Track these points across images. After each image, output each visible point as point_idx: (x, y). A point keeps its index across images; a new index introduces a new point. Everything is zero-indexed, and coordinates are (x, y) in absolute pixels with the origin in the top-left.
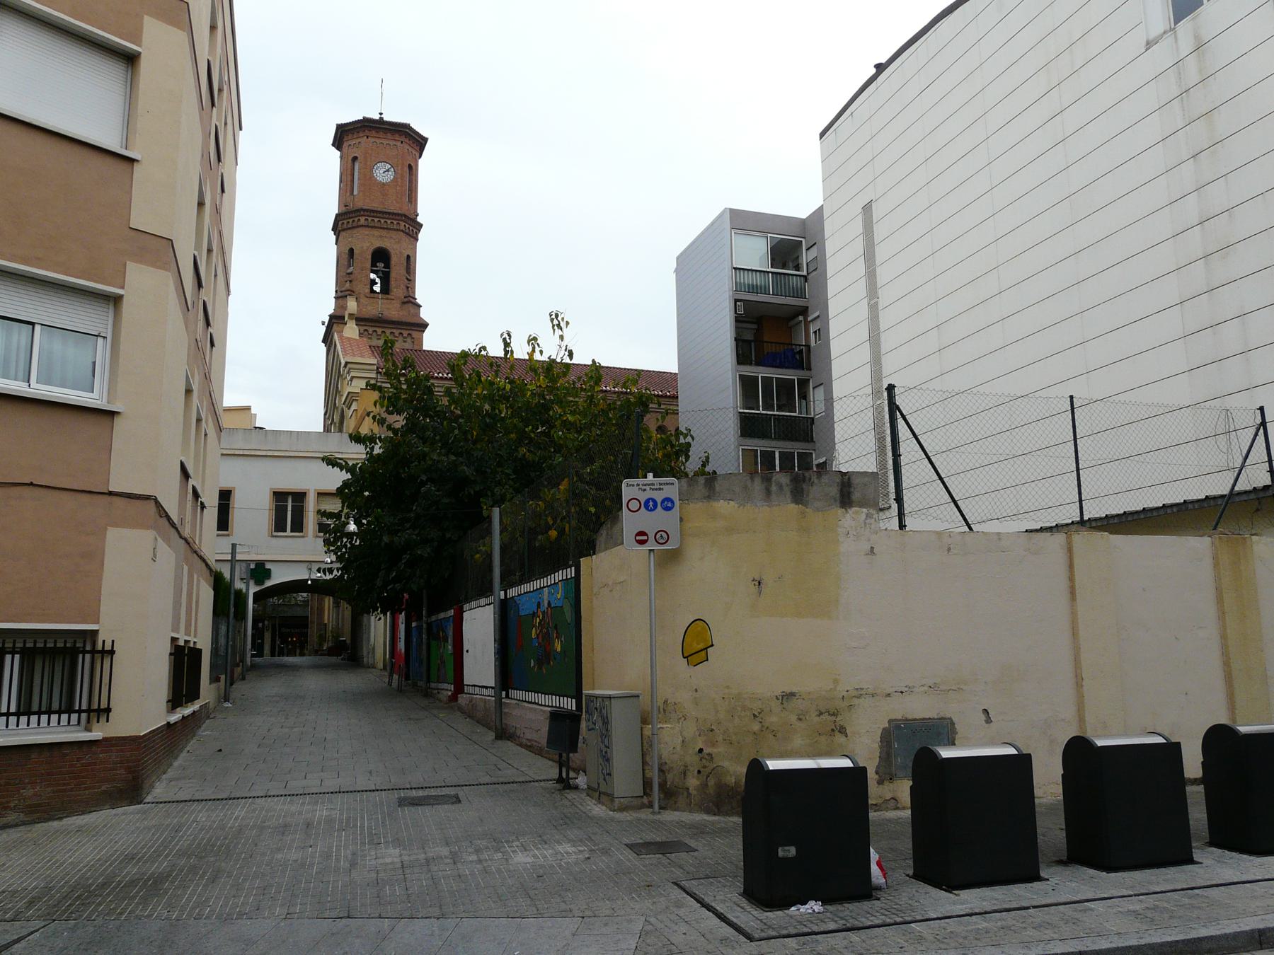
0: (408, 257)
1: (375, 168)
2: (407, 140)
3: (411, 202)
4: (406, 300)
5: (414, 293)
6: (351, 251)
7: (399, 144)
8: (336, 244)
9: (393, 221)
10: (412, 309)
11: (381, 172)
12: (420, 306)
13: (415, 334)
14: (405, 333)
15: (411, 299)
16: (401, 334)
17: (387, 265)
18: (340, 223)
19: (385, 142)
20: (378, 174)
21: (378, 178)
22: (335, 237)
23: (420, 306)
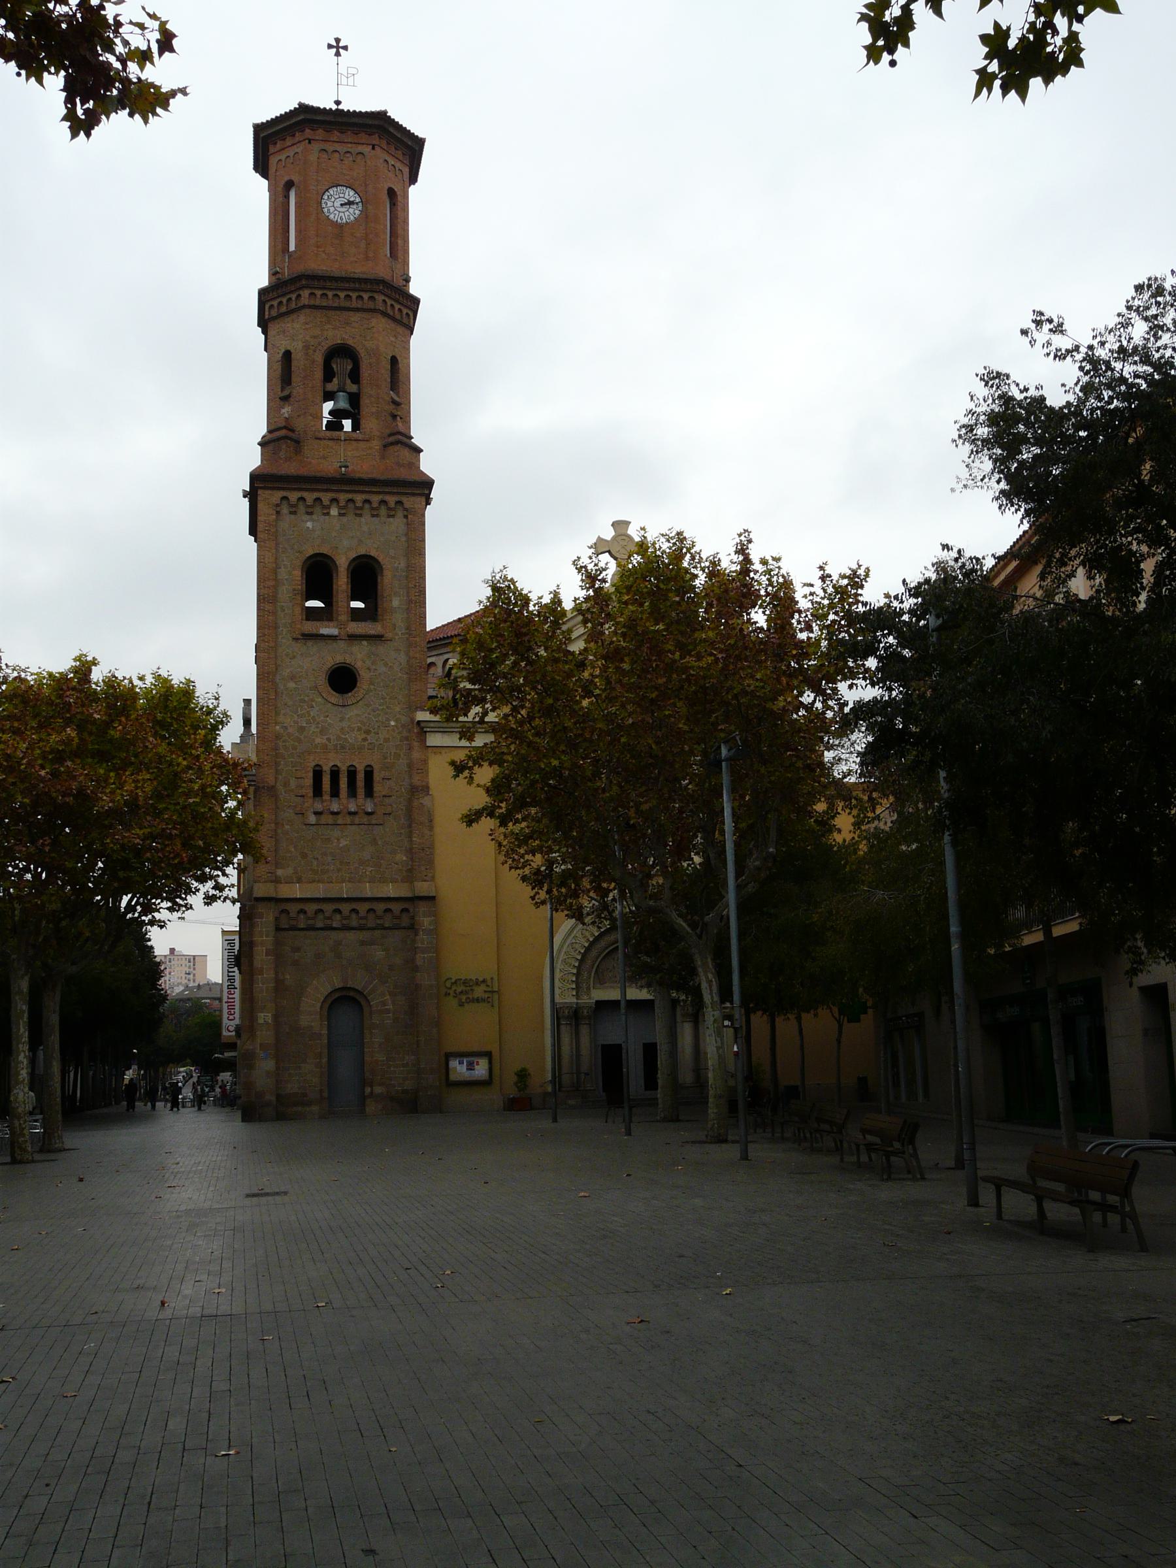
0: (394, 361)
1: (325, 197)
4: (392, 439)
6: (287, 355)
7: (366, 149)
8: (266, 350)
9: (362, 294)
10: (406, 453)
11: (337, 204)
12: (418, 451)
13: (408, 502)
14: (392, 500)
15: (400, 437)
16: (383, 502)
17: (355, 376)
19: (341, 148)
20: (332, 209)
21: (332, 217)
22: (263, 336)
23: (418, 451)
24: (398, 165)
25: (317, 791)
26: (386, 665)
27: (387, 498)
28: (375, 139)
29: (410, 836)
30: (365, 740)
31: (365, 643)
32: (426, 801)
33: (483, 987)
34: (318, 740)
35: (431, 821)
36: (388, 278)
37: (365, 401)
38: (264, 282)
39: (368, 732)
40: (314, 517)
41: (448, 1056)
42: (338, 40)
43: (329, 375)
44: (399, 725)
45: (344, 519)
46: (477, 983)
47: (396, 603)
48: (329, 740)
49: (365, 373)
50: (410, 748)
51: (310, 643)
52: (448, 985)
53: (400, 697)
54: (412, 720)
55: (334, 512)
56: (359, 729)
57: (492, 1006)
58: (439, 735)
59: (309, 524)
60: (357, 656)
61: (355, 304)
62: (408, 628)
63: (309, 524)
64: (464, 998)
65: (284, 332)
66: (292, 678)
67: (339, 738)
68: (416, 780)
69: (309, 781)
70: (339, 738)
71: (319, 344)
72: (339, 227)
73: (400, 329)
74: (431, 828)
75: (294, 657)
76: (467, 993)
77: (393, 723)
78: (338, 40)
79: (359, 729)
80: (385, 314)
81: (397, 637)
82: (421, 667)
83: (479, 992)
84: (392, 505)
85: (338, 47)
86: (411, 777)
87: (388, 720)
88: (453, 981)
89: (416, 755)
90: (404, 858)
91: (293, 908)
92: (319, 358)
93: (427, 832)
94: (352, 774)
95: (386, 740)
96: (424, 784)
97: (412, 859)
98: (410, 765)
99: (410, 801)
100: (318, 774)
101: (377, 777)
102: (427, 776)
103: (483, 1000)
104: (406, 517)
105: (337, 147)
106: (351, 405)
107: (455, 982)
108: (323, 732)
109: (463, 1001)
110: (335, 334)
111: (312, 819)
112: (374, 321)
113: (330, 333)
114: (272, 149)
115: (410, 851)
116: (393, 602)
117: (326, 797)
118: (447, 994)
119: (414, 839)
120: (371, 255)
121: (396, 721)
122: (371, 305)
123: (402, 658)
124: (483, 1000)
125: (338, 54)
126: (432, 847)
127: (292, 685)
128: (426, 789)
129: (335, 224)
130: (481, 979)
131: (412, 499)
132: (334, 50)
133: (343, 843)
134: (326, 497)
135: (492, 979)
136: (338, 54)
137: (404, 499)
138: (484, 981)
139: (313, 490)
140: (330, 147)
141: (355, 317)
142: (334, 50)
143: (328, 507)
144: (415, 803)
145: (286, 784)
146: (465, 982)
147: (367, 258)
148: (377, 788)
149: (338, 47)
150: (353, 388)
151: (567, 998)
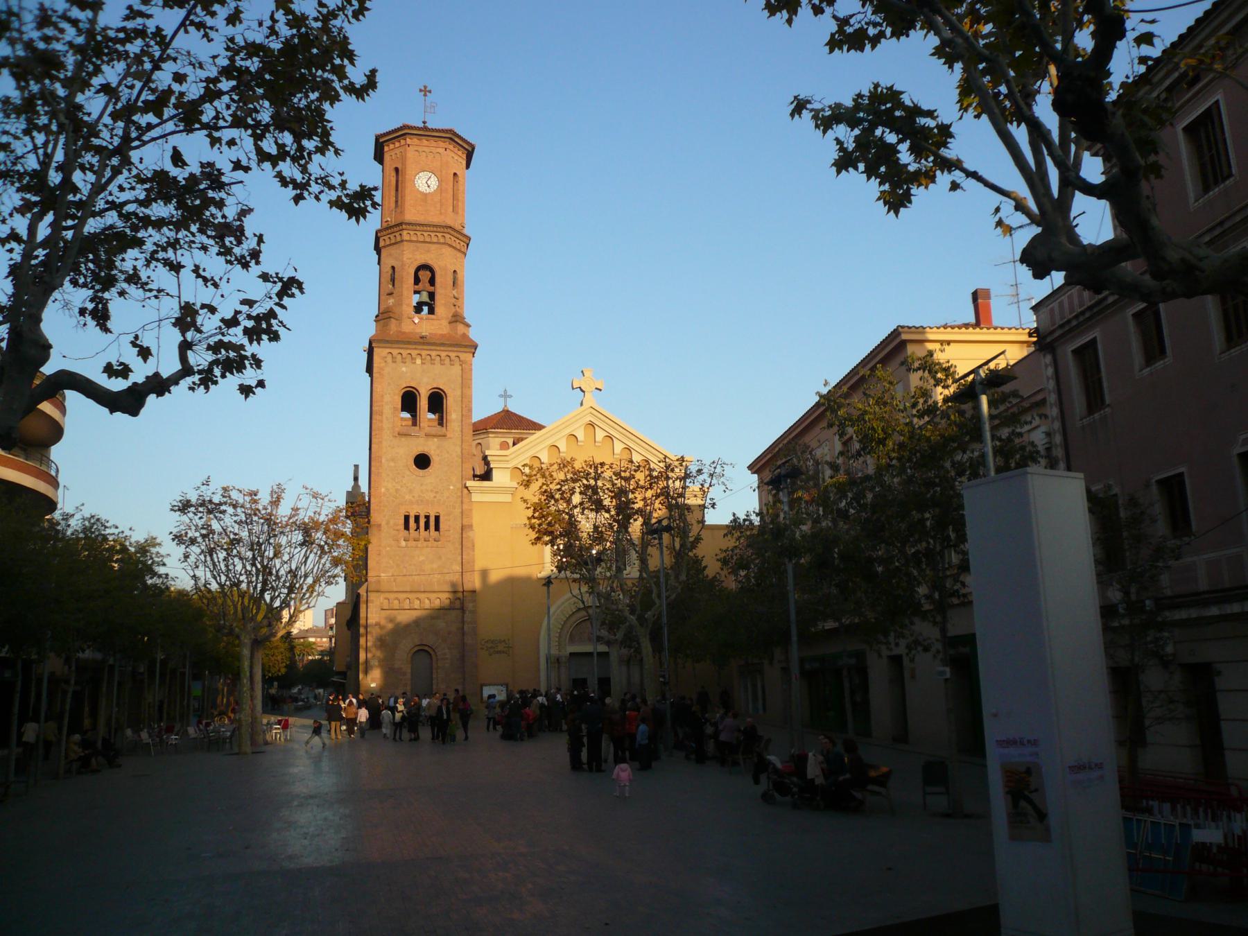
2: (451, 147)
3: (457, 213)
5: (462, 309)
7: (442, 151)
13: (463, 356)
17: (432, 282)
18: (381, 240)
21: (420, 189)
23: (468, 326)
24: (460, 160)
25: (407, 527)
26: (448, 452)
27: (450, 354)
28: (446, 145)
30: (435, 497)
31: (436, 440)
32: (470, 534)
34: (407, 497)
35: (474, 546)
36: (452, 225)
37: (437, 297)
38: (379, 227)
39: (437, 492)
40: (407, 364)
41: (482, 686)
42: (425, 87)
43: (417, 280)
45: (425, 366)
46: (500, 642)
48: (413, 497)
49: (438, 280)
51: (403, 439)
52: (483, 643)
55: (419, 361)
56: (432, 491)
59: (404, 369)
60: (430, 447)
61: (435, 240)
63: (404, 369)
65: (390, 255)
66: (393, 460)
67: (419, 496)
69: (402, 521)
70: (419, 496)
71: (412, 263)
72: (425, 196)
73: (459, 255)
74: (474, 551)
75: (393, 448)
77: (452, 487)
78: (425, 87)
79: (432, 491)
80: (451, 246)
83: (500, 648)
84: (453, 358)
85: (425, 91)
91: (391, 596)
92: (412, 272)
94: (427, 517)
95: (448, 498)
100: (407, 518)
101: (441, 518)
103: (503, 652)
104: (461, 365)
105: (425, 149)
106: (430, 298)
108: (411, 491)
110: (422, 259)
111: (403, 543)
112: (444, 250)
113: (418, 257)
114: (386, 149)
117: (412, 531)
118: (483, 649)
120: (443, 211)
122: (442, 240)
123: (459, 450)
124: (503, 652)
125: (425, 95)
126: (474, 562)
127: (392, 464)
128: (470, 527)
129: (422, 193)
131: (465, 355)
132: (423, 93)
133: (422, 558)
134: (414, 353)
136: (425, 95)
137: (460, 354)
139: (407, 349)
140: (420, 149)
141: (433, 247)
142: (423, 93)
143: (415, 359)
145: (388, 523)
146: (493, 642)
147: (441, 214)
148: (441, 526)
149: (425, 91)
150: (431, 289)
151: (554, 652)
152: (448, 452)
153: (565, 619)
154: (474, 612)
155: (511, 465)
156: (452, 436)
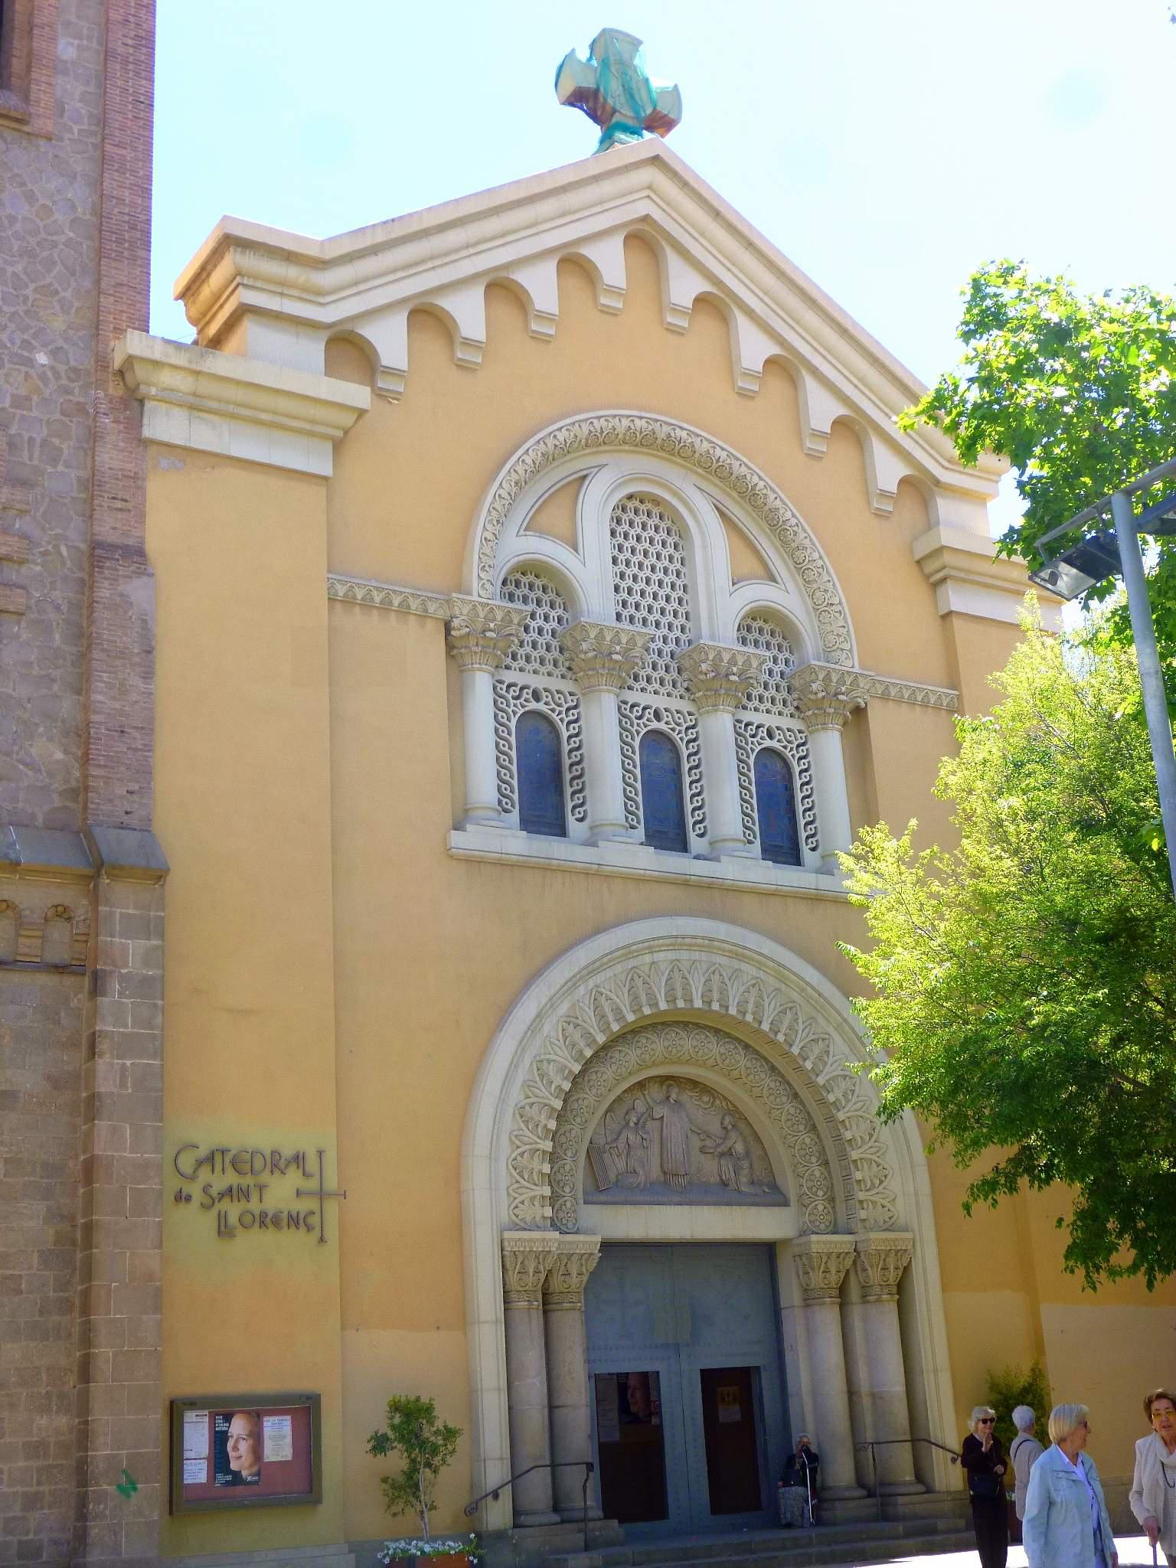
26: (30, 197)
29: (82, 685)
32: (135, 589)
33: (293, 1179)
41: (175, 1411)
44: (62, 368)
46: (276, 1163)
47: (67, 49)
50: (93, 437)
52: (187, 1163)
53: (68, 294)
54: (102, 361)
57: (322, 1240)
58: (180, 415)
62: (102, 121)
64: (234, 1210)
68: (108, 528)
74: (148, 675)
76: (244, 1194)
81: (67, 136)
82: (133, 228)
86: (90, 517)
87: (26, 345)
88: (203, 1152)
89: (111, 457)
90: (59, 755)
93: (137, 681)
96: (131, 542)
97: (85, 760)
98: (92, 485)
99: (86, 586)
102: (141, 517)
103: (294, 1221)
107: (210, 1159)
109: (233, 1219)
115: (82, 737)
116: (62, 43)
118: (182, 1198)
119: (100, 697)
121: (55, 353)
123: (80, 194)
124: (294, 1221)
126: (148, 729)
128: (136, 555)
130: (288, 1153)
135: (320, 1153)
138: (298, 1159)
144: (104, 592)
152: (30, 197)
153: (577, 1068)
154: (152, 988)
155: (330, 314)
156: (49, 126)
